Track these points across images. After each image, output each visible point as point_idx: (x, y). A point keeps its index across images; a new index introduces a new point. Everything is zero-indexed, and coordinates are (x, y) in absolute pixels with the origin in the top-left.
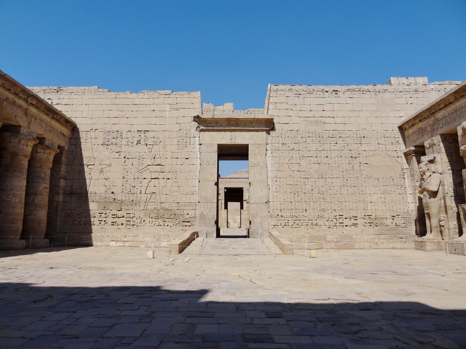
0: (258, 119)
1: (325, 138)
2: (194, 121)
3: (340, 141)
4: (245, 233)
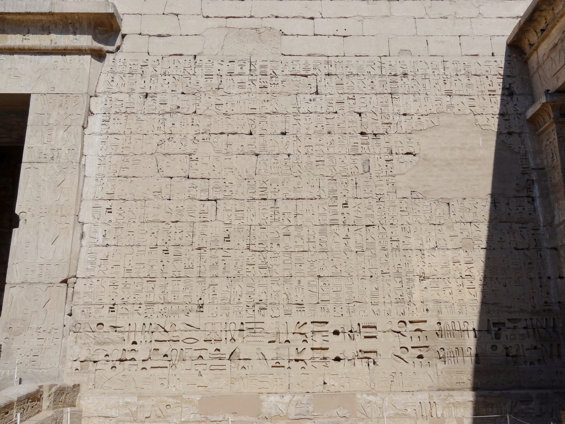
1: (280, 78)
3: (328, 86)
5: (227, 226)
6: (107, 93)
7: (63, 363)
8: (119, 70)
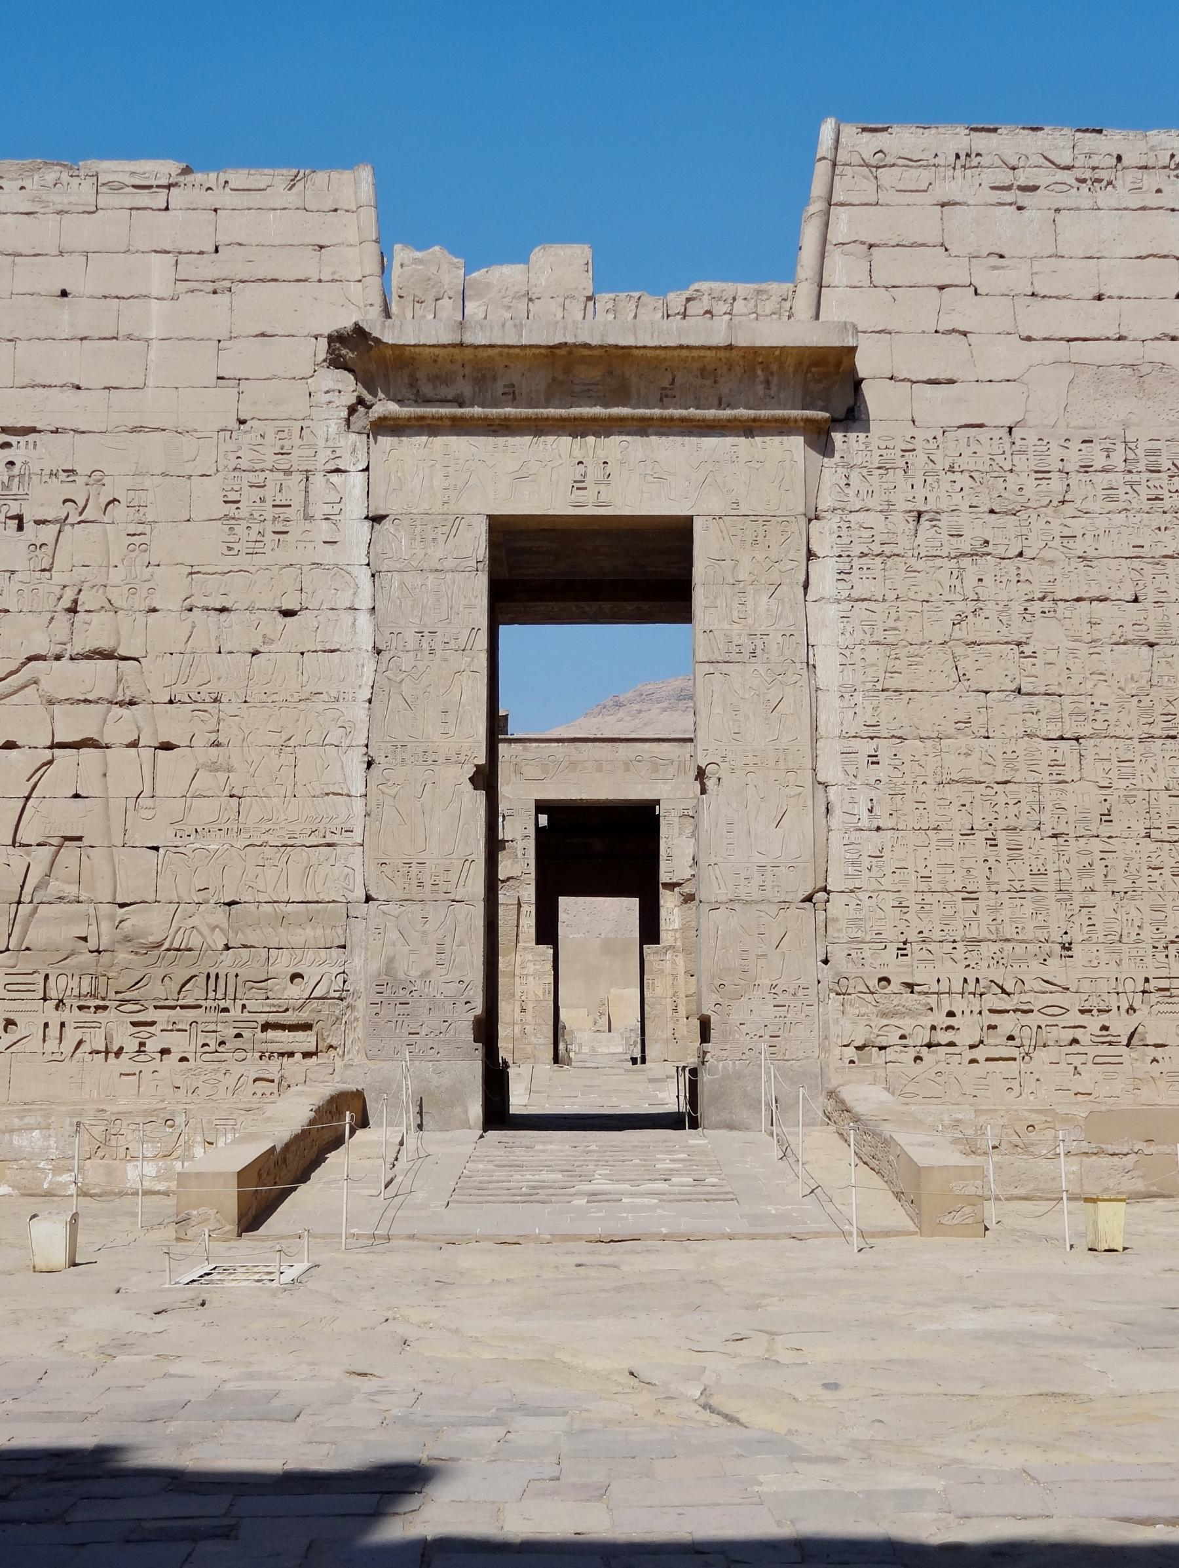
0: (755, 351)
2: (336, 362)
4: (670, 1099)
5: (1103, 791)
6: (839, 512)
7: (823, 1049)
8: (858, 460)
